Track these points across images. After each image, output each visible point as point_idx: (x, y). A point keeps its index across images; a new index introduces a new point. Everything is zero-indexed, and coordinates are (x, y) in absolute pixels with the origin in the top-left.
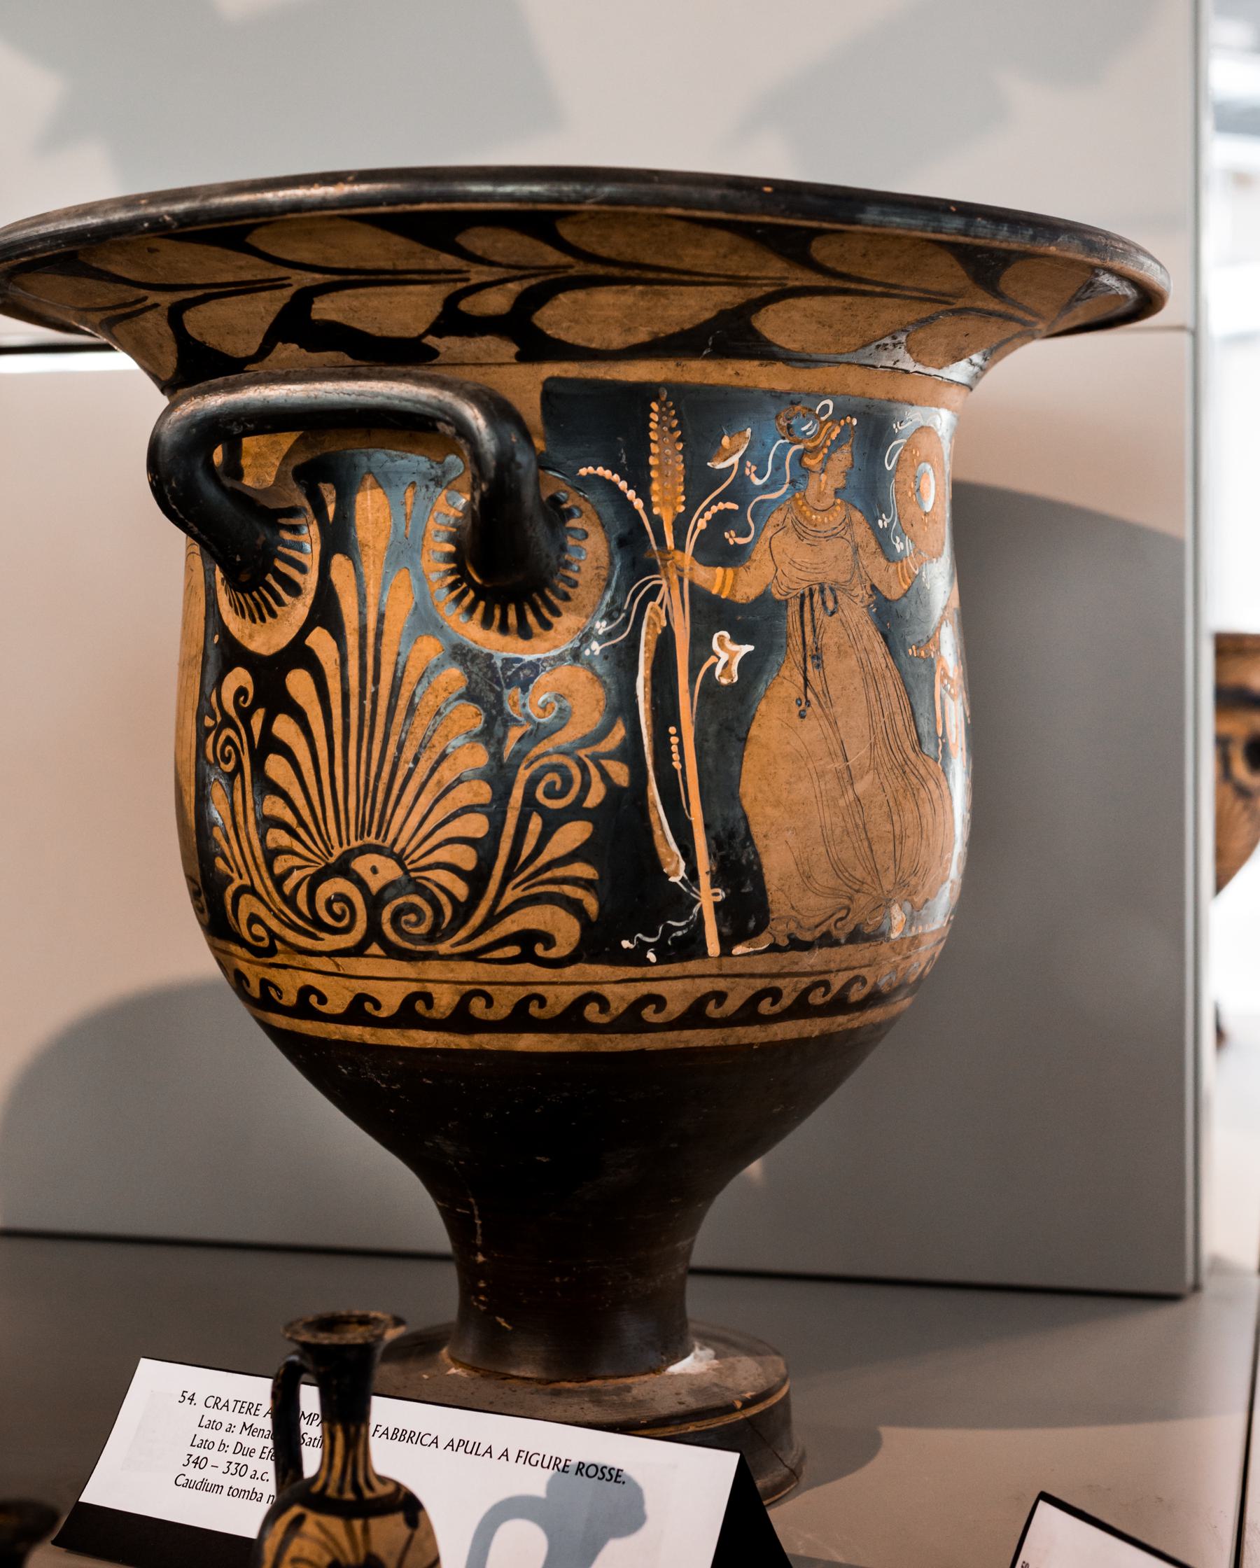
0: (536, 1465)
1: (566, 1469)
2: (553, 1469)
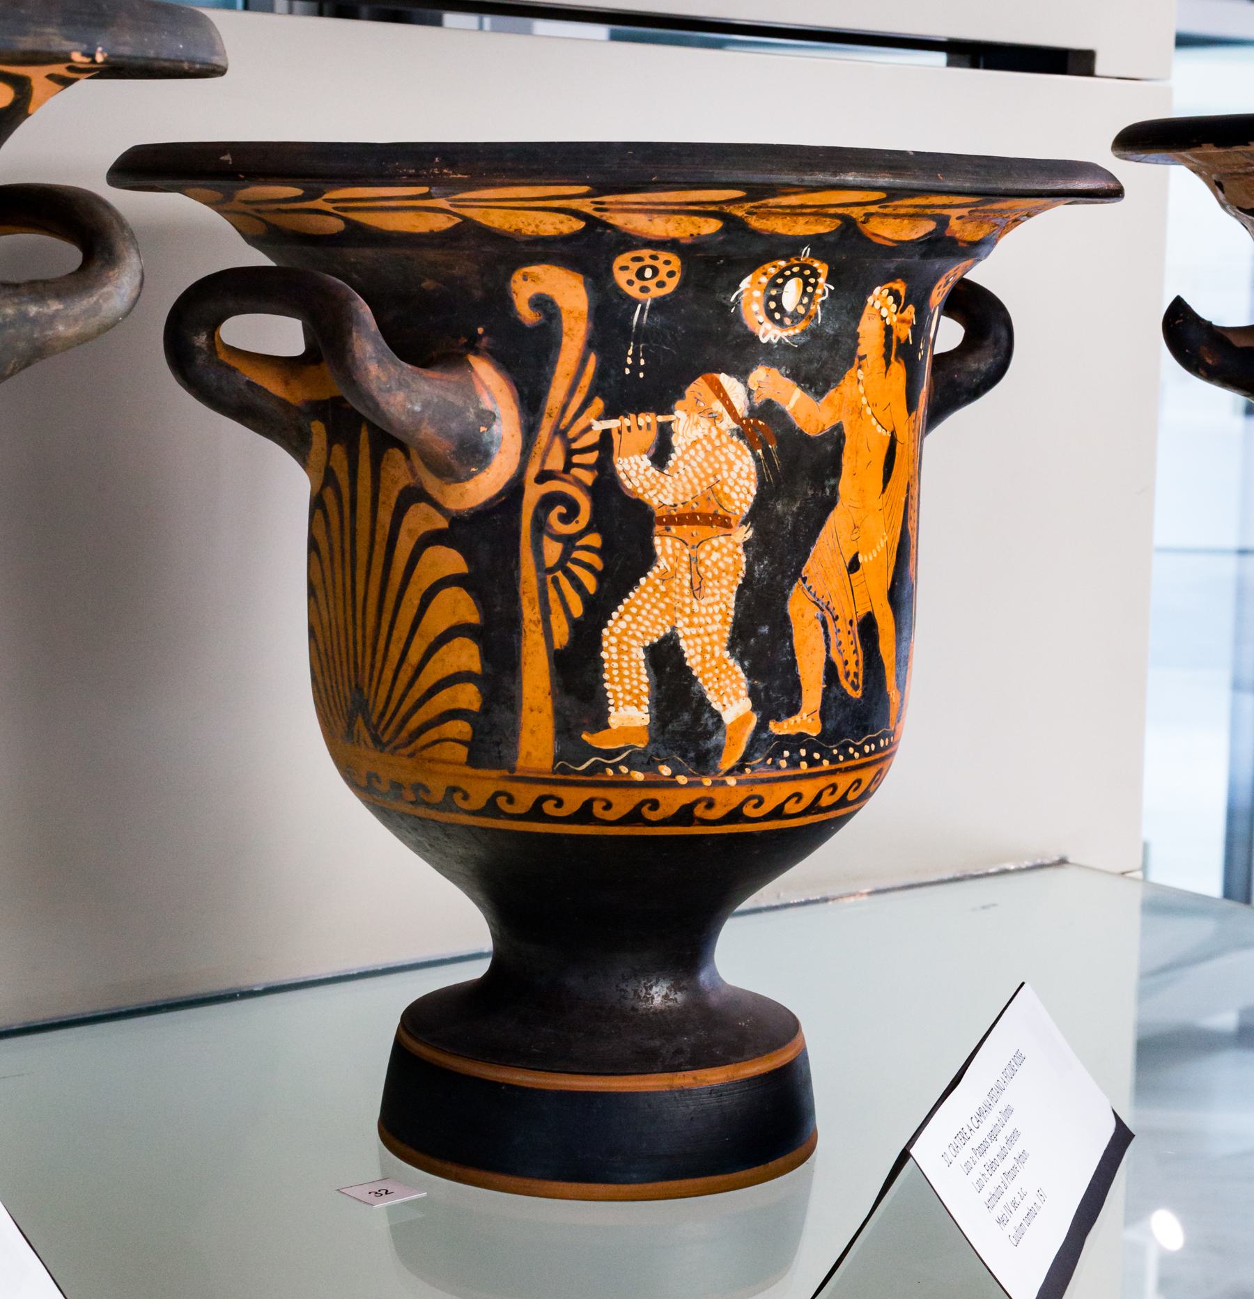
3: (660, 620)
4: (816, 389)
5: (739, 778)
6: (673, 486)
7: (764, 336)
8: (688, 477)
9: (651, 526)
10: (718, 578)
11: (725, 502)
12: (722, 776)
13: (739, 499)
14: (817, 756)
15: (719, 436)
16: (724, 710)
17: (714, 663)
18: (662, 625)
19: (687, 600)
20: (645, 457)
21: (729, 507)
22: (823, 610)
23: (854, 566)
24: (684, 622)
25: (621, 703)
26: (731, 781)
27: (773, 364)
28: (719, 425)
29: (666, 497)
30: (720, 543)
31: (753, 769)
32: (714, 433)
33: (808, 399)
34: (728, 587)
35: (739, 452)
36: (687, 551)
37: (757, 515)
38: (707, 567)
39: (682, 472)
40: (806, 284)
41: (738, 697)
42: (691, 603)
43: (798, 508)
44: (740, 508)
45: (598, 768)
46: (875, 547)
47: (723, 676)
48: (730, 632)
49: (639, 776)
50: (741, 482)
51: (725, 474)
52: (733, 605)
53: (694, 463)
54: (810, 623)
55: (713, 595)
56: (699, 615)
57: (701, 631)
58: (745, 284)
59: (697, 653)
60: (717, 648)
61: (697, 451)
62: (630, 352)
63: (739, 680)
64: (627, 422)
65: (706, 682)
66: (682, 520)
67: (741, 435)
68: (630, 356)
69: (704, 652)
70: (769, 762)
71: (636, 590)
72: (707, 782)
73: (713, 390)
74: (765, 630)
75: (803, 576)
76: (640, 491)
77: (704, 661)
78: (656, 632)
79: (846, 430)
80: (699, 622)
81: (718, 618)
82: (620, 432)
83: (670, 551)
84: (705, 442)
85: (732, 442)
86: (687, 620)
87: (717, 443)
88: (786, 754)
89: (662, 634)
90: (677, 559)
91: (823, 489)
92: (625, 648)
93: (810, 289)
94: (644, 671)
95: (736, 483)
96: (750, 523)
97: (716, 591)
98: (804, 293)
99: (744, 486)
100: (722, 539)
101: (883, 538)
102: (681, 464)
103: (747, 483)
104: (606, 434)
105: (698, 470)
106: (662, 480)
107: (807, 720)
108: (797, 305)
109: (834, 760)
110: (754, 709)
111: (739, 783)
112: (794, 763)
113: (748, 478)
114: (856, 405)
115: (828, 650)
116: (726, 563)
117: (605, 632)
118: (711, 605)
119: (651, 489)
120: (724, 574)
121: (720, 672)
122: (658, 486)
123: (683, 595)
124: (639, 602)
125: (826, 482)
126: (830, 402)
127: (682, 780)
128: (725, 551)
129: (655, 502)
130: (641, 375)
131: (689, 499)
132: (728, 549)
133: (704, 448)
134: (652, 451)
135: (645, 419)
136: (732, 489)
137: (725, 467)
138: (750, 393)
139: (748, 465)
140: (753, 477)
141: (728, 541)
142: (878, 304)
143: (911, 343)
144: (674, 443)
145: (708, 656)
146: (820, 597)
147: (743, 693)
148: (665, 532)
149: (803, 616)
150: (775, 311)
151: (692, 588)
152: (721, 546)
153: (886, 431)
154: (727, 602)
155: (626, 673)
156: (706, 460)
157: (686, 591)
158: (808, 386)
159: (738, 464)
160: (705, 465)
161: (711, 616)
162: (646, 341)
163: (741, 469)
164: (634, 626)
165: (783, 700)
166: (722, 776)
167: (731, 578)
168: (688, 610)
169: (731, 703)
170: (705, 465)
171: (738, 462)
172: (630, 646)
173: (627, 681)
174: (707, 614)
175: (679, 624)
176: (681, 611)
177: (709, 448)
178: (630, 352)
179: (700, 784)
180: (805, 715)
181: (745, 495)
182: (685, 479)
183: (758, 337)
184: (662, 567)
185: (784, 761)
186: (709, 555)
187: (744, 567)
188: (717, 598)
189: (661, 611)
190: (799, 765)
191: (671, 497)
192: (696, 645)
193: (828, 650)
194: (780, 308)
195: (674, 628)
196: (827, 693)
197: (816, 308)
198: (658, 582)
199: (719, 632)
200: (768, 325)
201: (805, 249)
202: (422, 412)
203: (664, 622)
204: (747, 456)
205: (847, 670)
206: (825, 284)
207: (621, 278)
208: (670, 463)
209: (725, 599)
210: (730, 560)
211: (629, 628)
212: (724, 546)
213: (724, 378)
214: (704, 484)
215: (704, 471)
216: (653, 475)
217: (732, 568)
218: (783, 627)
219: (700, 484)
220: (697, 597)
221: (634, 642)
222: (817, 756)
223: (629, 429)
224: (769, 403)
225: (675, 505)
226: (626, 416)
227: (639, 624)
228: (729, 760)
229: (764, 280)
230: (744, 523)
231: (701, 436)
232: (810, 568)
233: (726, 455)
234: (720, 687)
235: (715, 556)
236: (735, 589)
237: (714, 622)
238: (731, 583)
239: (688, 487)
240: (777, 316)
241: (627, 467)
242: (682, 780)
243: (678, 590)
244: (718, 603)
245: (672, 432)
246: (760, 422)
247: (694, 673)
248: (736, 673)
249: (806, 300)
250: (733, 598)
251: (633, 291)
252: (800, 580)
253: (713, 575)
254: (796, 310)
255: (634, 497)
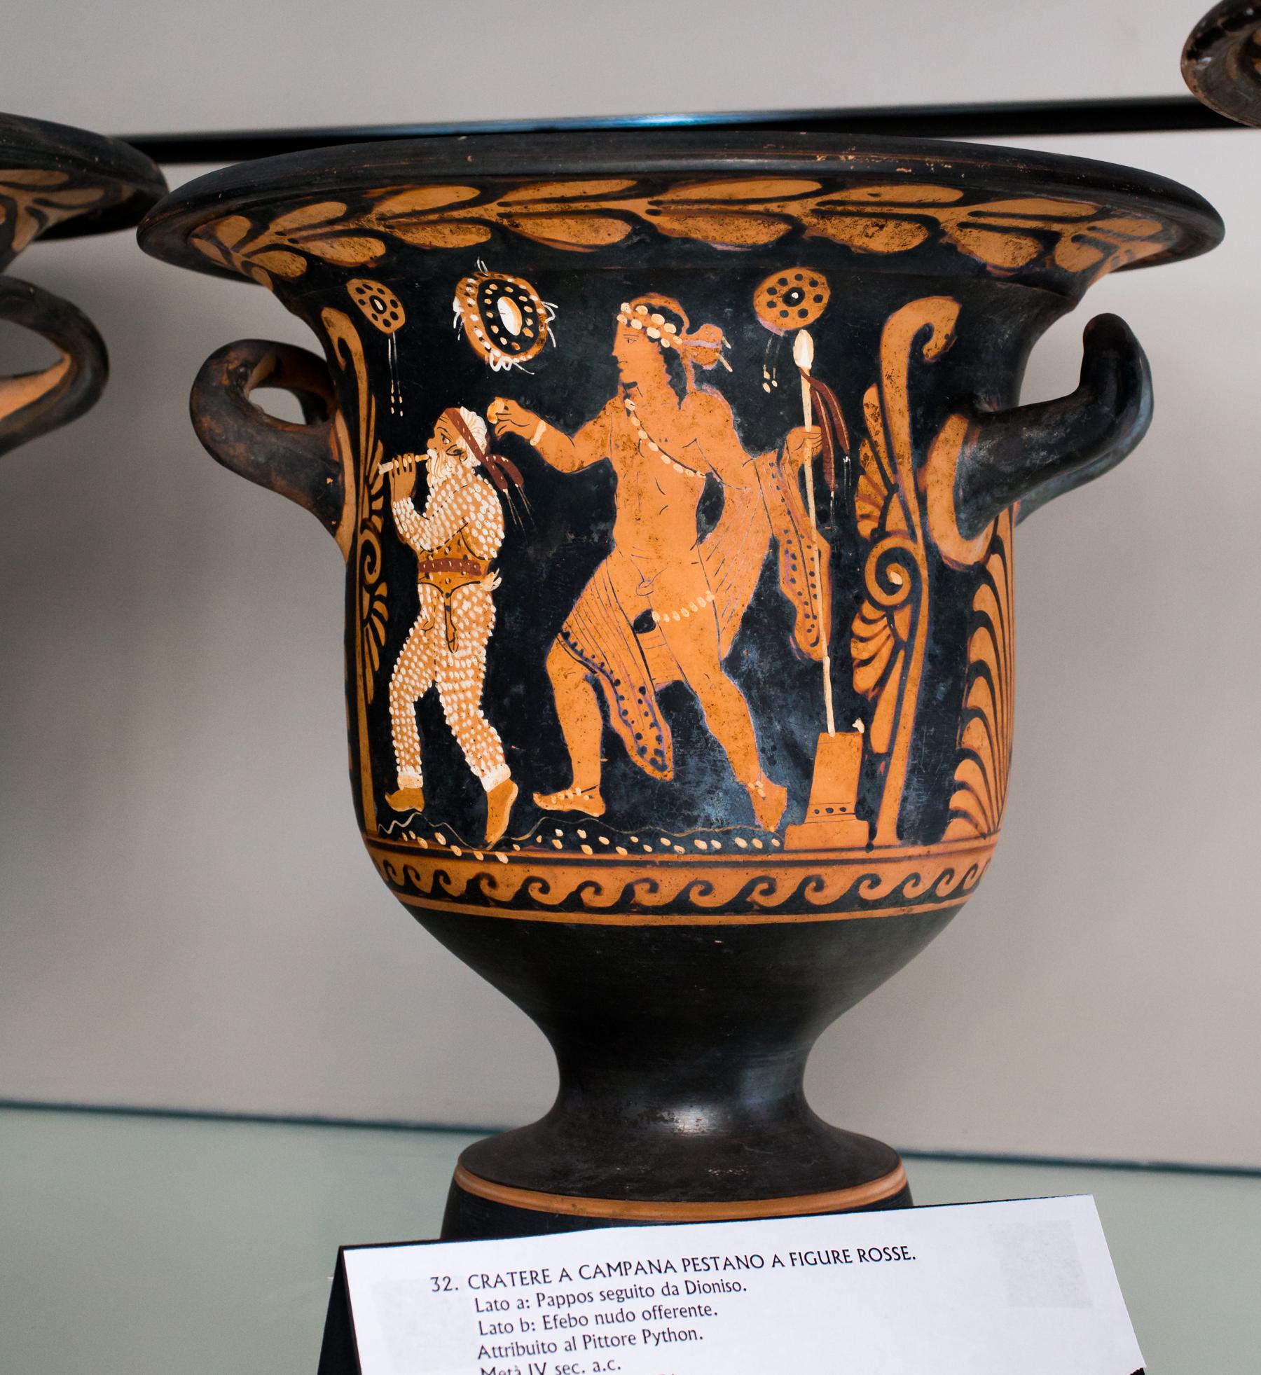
0: (816, 1263)
1: (848, 1259)
2: (835, 1262)
3: (424, 674)
4: (565, 422)
5: (510, 854)
6: (430, 529)
7: (495, 364)
8: (441, 520)
9: (416, 572)
10: (467, 629)
11: (474, 547)
12: (491, 851)
13: (487, 544)
14: (604, 841)
15: (464, 475)
16: (483, 775)
17: (469, 722)
18: (426, 679)
19: (444, 653)
20: (410, 499)
21: (478, 553)
22: (595, 672)
23: (644, 623)
24: (442, 677)
25: (403, 763)
26: (503, 857)
27: (507, 395)
28: (464, 463)
29: (425, 542)
30: (470, 591)
31: (521, 844)
32: (461, 471)
33: (558, 435)
34: (479, 640)
35: (485, 492)
36: (442, 600)
37: (505, 561)
38: (459, 617)
39: (436, 515)
40: (521, 305)
41: (495, 763)
42: (447, 656)
43: (554, 554)
44: (488, 553)
45: (398, 831)
46: (686, 605)
47: (479, 738)
48: (483, 690)
49: (423, 843)
50: (488, 525)
51: (473, 516)
52: (484, 660)
53: (445, 505)
54: (577, 686)
55: (466, 647)
56: (454, 669)
57: (457, 687)
58: (457, 307)
59: (454, 711)
60: (471, 706)
61: (447, 492)
62: (392, 391)
63: (494, 742)
64: (397, 464)
65: (464, 742)
66: (442, 564)
67: (482, 470)
68: (393, 395)
69: (460, 710)
70: (539, 839)
71: (408, 641)
72: (479, 856)
73: (456, 425)
74: (520, 689)
75: (564, 631)
76: (408, 536)
77: (460, 721)
78: (422, 687)
79: (617, 467)
80: (454, 677)
81: (471, 673)
82: (393, 476)
83: (429, 600)
84: (453, 482)
85: (477, 480)
86: (444, 674)
87: (464, 483)
88: (559, 832)
89: (426, 689)
90: (435, 608)
91: (589, 534)
92: (402, 703)
93: (528, 309)
94: (416, 729)
95: (484, 526)
96: (498, 570)
97: (468, 643)
98: (525, 315)
99: (491, 529)
100: (472, 587)
101: (704, 596)
102: (435, 506)
103: (494, 526)
104: (386, 475)
105: (449, 512)
106: (422, 523)
107: (582, 797)
108: (522, 328)
109: (632, 848)
110: (513, 778)
111: (512, 860)
112: (572, 844)
113: (495, 520)
114: (630, 440)
115: (606, 717)
116: (476, 613)
117: (391, 685)
118: (463, 658)
119: (415, 534)
120: (474, 625)
121: (476, 734)
122: (420, 531)
123: (440, 647)
124: (409, 654)
125: (592, 527)
126: (588, 436)
127: (457, 851)
128: (475, 599)
129: (418, 549)
130: (401, 414)
131: (442, 544)
132: (478, 598)
133: (452, 487)
134: (414, 493)
135: (409, 460)
136: (480, 532)
137: (472, 508)
138: (490, 427)
139: (495, 506)
140: (500, 519)
141: (477, 589)
142: (637, 325)
143: (731, 370)
144: (430, 485)
145: (464, 715)
146: (589, 657)
147: (501, 758)
148: (425, 580)
149: (566, 677)
150: (499, 335)
151: (447, 639)
152: (472, 594)
153: (695, 472)
154: (479, 655)
155: (405, 730)
156: (455, 501)
157: (443, 643)
158: (554, 417)
159: (485, 505)
160: (455, 506)
161: (464, 670)
162: (400, 379)
163: (488, 511)
164: (407, 680)
165: (548, 770)
166: (491, 851)
167: (481, 630)
168: (444, 663)
169: (489, 768)
170: (455, 506)
171: (484, 502)
172: (406, 701)
173: (405, 738)
174: (461, 669)
175: (438, 679)
176: (440, 665)
177: (457, 488)
178: (392, 391)
179: (474, 859)
180: (578, 791)
181: (493, 539)
182: (439, 522)
183: (489, 365)
184: (424, 618)
185: (558, 841)
186: (461, 604)
187: (494, 618)
188: (469, 651)
189: (425, 664)
190: (581, 849)
191: (429, 542)
192: (452, 701)
193: (606, 717)
194: (504, 332)
195: (434, 682)
196: (609, 769)
197: (545, 330)
198: (422, 632)
199: (473, 689)
200: (496, 352)
201: (478, 262)
202: (267, 463)
203: (427, 676)
204: (493, 496)
205: (641, 746)
206: (543, 303)
207: (368, 311)
208: (427, 505)
209: (476, 653)
210: (479, 610)
211: (404, 683)
212: (475, 595)
213: (463, 411)
214: (455, 527)
215: (454, 514)
216: (416, 518)
217: (482, 619)
218: (542, 689)
219: (451, 528)
220: (452, 647)
221: (408, 698)
222: (604, 841)
223: (398, 469)
224: (510, 436)
225: (432, 551)
226: (396, 459)
227: (411, 678)
228: (495, 834)
229: (472, 301)
230: (492, 568)
231: (450, 476)
232: (573, 622)
233: (472, 495)
234: (477, 750)
235: (466, 605)
236: (486, 642)
237: (467, 678)
238: (481, 635)
239: (442, 530)
240: (504, 341)
241: (399, 513)
242: (457, 851)
243: (436, 642)
244: (469, 657)
245: (427, 473)
246: (504, 459)
247: (454, 733)
248: (492, 736)
249: (530, 322)
250: (484, 652)
251: (379, 325)
252: (560, 636)
253: (465, 625)
254: (522, 333)
255: (404, 543)
